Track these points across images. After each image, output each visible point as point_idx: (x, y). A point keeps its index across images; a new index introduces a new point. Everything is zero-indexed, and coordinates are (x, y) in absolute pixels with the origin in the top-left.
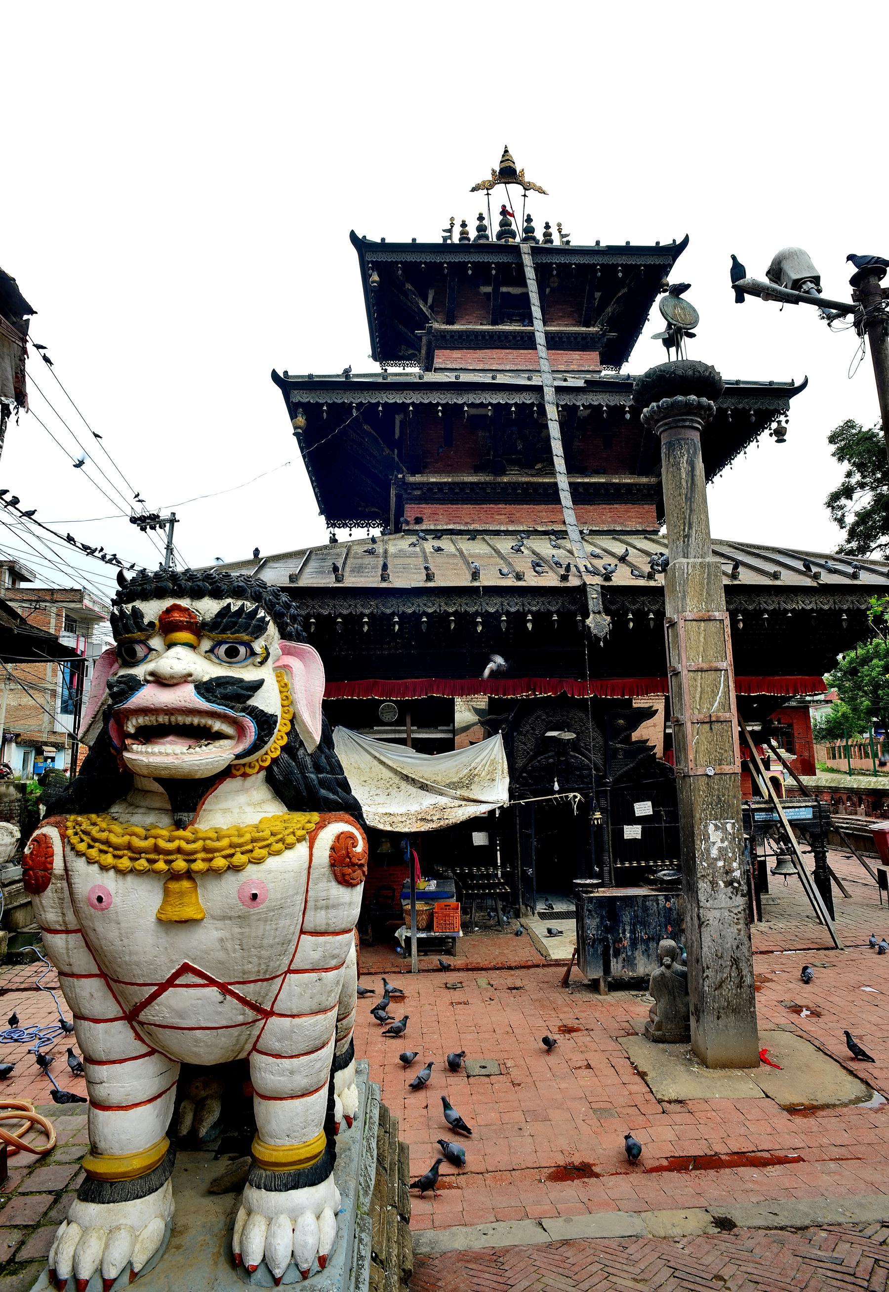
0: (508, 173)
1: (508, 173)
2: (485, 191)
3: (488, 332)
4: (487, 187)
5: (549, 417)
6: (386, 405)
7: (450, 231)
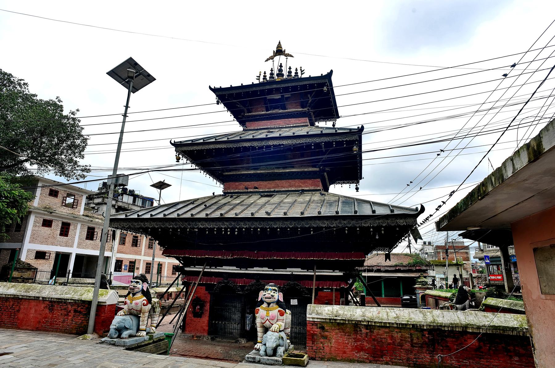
0: (279, 52)
1: (279, 52)
4: (272, 58)
7: (259, 77)
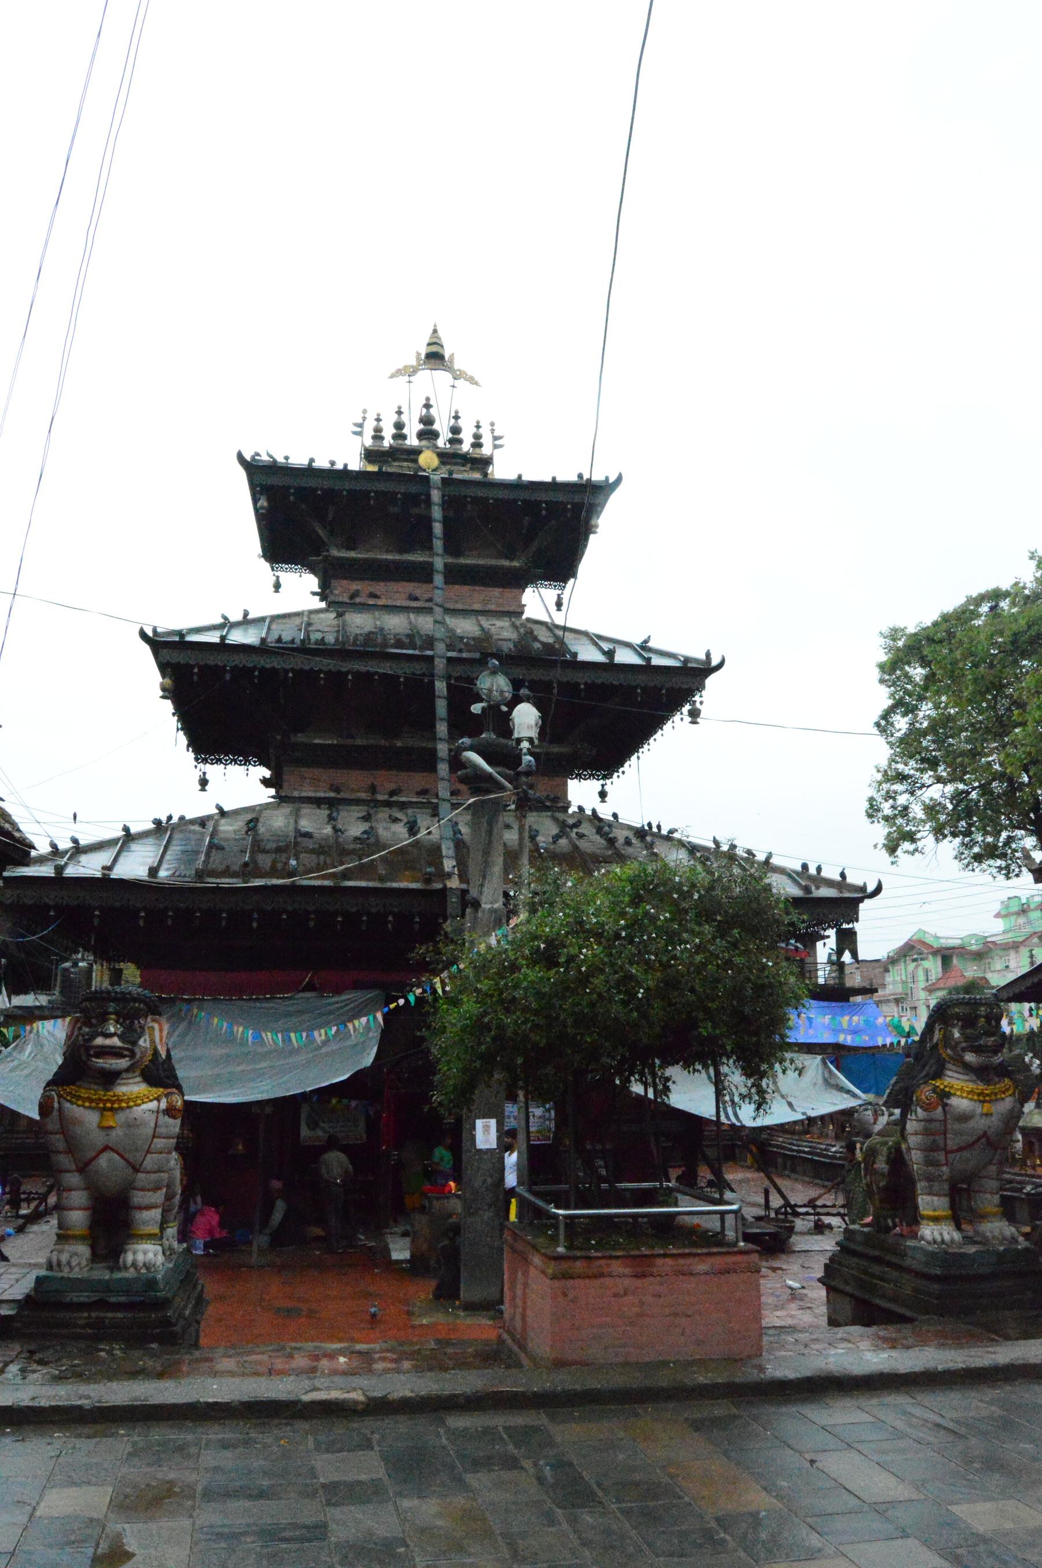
0: (435, 357)
2: (407, 378)
3: (394, 562)
5: (437, 694)
6: (263, 670)
7: (361, 426)
